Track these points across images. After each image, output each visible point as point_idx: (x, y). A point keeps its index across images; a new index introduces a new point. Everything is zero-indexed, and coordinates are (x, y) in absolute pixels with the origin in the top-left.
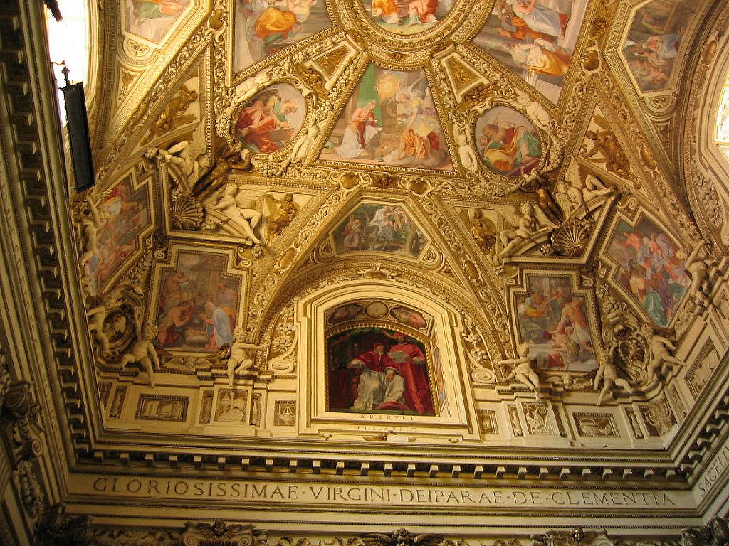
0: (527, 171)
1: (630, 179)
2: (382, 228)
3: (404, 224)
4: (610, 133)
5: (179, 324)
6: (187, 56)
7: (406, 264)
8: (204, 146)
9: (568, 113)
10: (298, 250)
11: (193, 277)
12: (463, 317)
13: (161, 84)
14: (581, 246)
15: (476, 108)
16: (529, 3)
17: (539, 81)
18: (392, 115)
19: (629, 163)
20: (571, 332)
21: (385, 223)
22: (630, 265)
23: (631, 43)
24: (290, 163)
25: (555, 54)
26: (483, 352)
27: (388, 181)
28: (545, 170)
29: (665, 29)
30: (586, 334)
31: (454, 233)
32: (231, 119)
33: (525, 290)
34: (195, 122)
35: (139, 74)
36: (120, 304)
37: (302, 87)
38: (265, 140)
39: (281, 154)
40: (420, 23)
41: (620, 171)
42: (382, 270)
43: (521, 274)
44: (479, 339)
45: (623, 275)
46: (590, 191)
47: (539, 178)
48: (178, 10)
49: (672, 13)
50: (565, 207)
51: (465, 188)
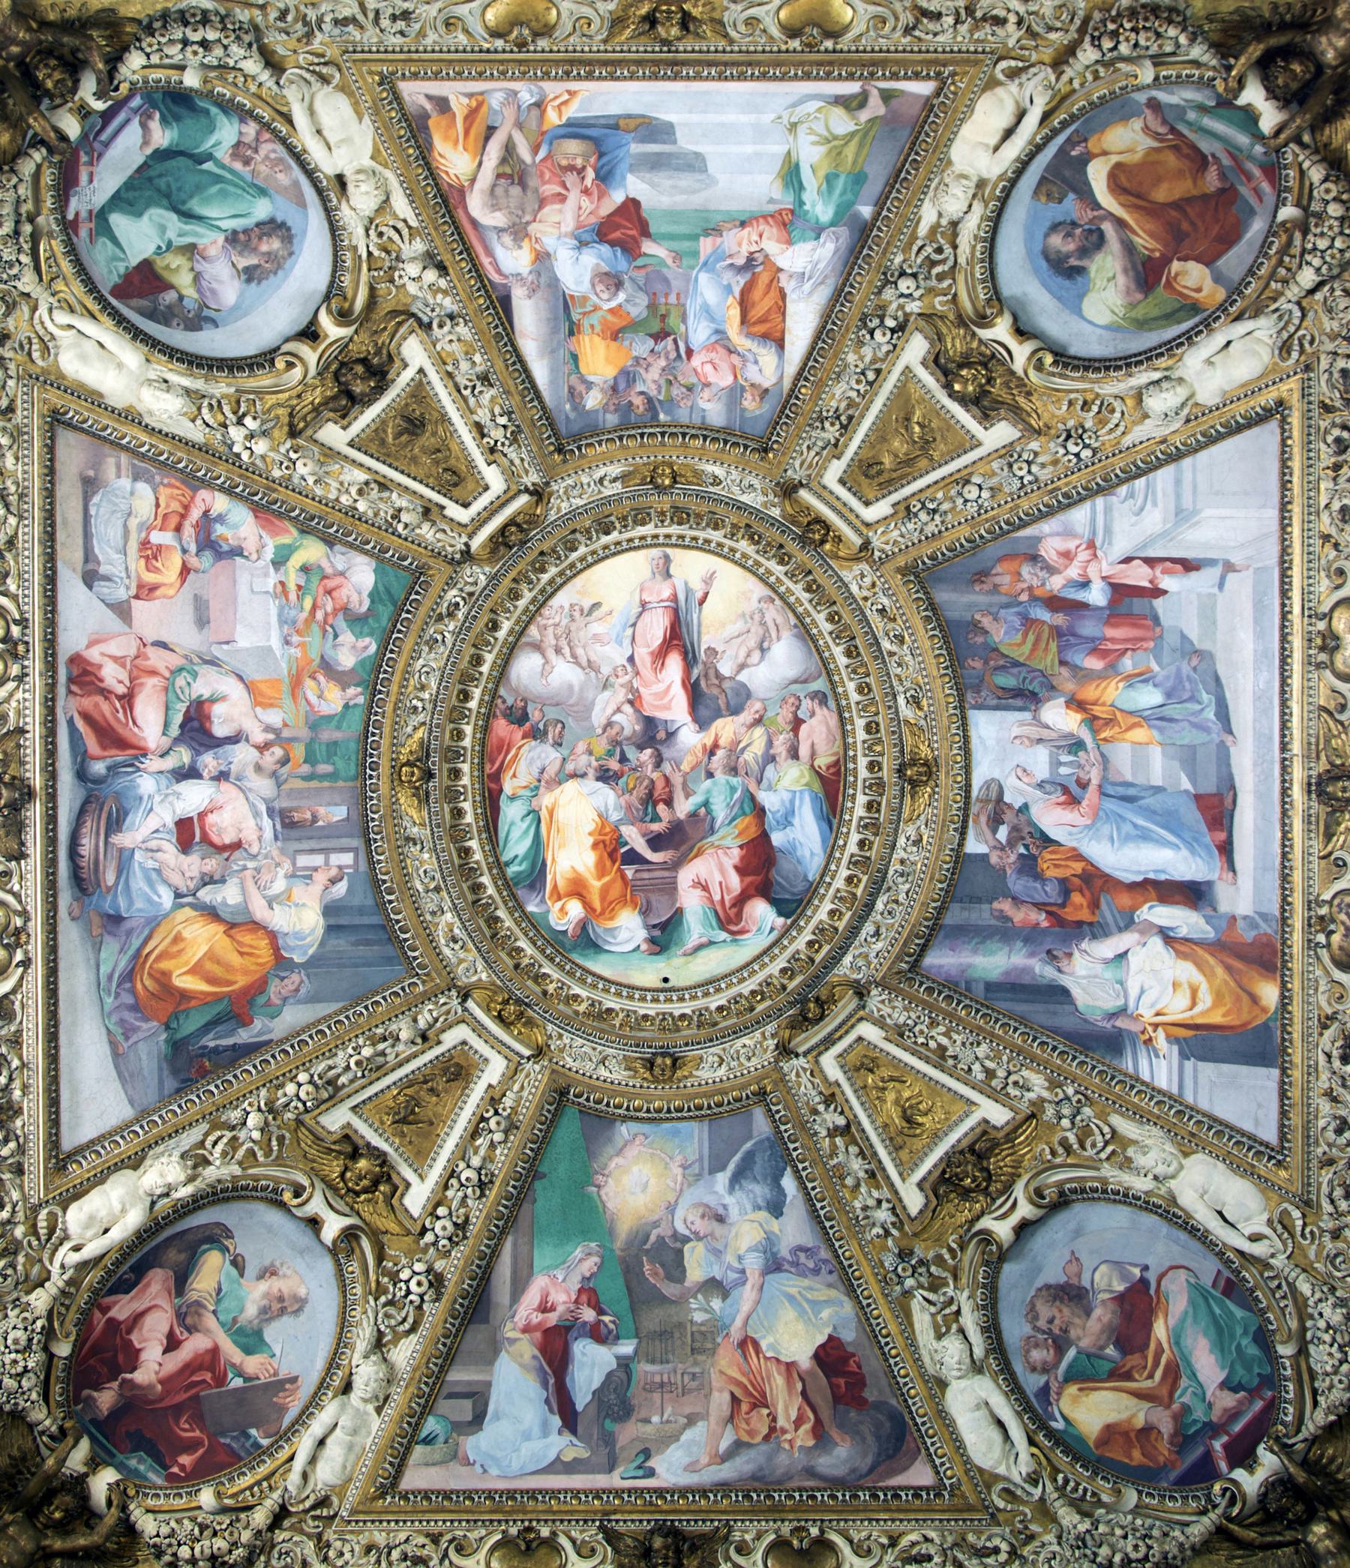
0: (1243, 1455)
15: (986, 1223)
17: (1189, 1065)
18: (669, 1289)
27: (678, 1552)
28: (1310, 1428)
37: (316, 1205)
39: (247, 1480)
40: (724, 935)
51: (996, 1551)
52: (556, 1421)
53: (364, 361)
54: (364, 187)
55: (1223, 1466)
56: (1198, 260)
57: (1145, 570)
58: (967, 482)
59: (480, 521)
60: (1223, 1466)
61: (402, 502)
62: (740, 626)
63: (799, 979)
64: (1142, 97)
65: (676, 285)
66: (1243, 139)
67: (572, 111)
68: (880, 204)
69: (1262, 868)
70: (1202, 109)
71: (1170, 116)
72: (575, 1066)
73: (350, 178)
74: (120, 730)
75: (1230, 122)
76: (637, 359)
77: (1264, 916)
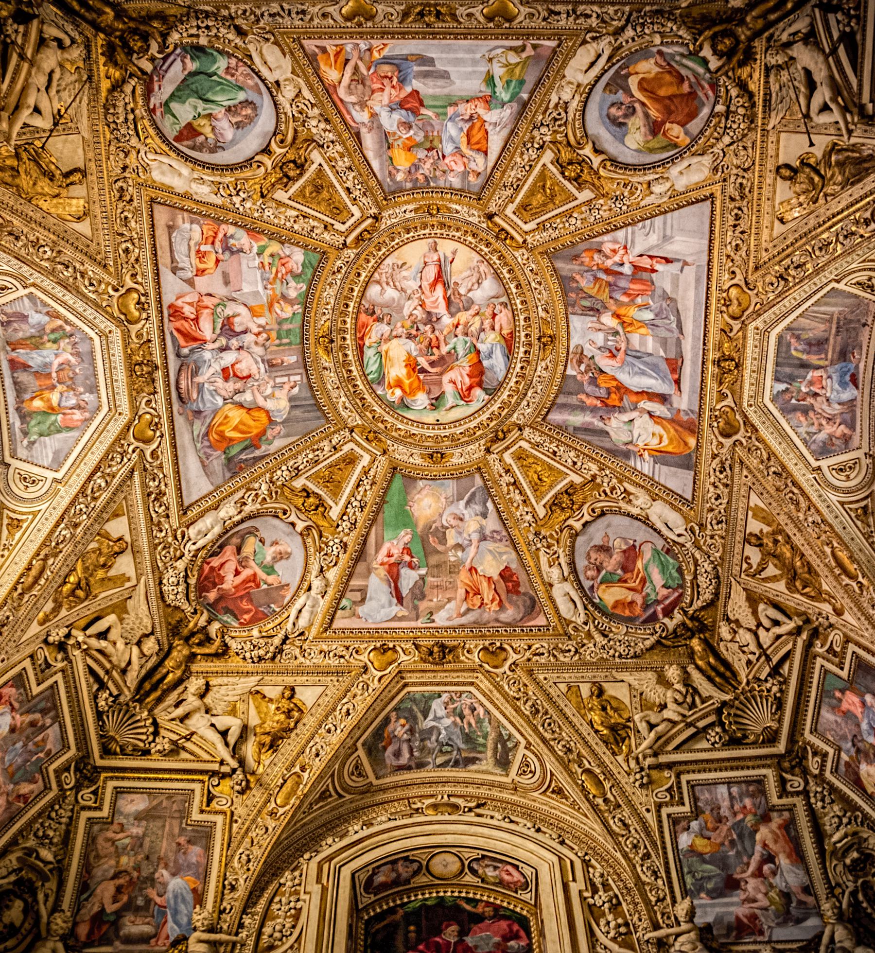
1: (825, 600)
2: (445, 729)
3: (479, 721)
4: (780, 531)
5: (110, 908)
6: (103, 484)
7: (492, 785)
8: (147, 622)
9: (711, 510)
10: (306, 775)
11: (137, 830)
12: (586, 864)
13: (66, 528)
14: (774, 725)
15: (571, 522)
16: (618, 350)
17: (657, 466)
18: (440, 548)
19: (819, 576)
20: (774, 873)
21: (448, 722)
22: (854, 745)
23: (782, 387)
24: (286, 638)
25: (672, 421)
26: (620, 921)
27: (444, 653)
28: (695, 606)
29: (830, 356)
30: (801, 873)
31: (559, 727)
32: (186, 577)
33: (686, 808)
34: (127, 585)
35: (31, 517)
36: (13, 878)
37: (293, 518)
38: (245, 605)
39: (271, 625)
40: (462, 402)
41: (807, 590)
42: (453, 800)
43: (679, 783)
44: (614, 901)
45: (847, 764)
46: (768, 630)
47: (688, 622)
48: (86, 420)
49: (834, 330)
50: (739, 664)
51: (569, 651)
52: (395, 601)
53: (294, 162)
54: (288, 88)
55: (661, 616)
56: (678, 123)
57: (649, 260)
58: (571, 216)
59: (350, 231)
60: (661, 616)
61: (316, 224)
62: (468, 273)
63: (494, 422)
64: (655, 50)
65: (437, 127)
66: (701, 70)
67: (385, 52)
68: (532, 93)
69: (692, 391)
70: (682, 55)
71: (668, 58)
72: (397, 456)
73: (282, 83)
74: (194, 334)
75: (695, 61)
76: (420, 160)
77: (692, 411)
